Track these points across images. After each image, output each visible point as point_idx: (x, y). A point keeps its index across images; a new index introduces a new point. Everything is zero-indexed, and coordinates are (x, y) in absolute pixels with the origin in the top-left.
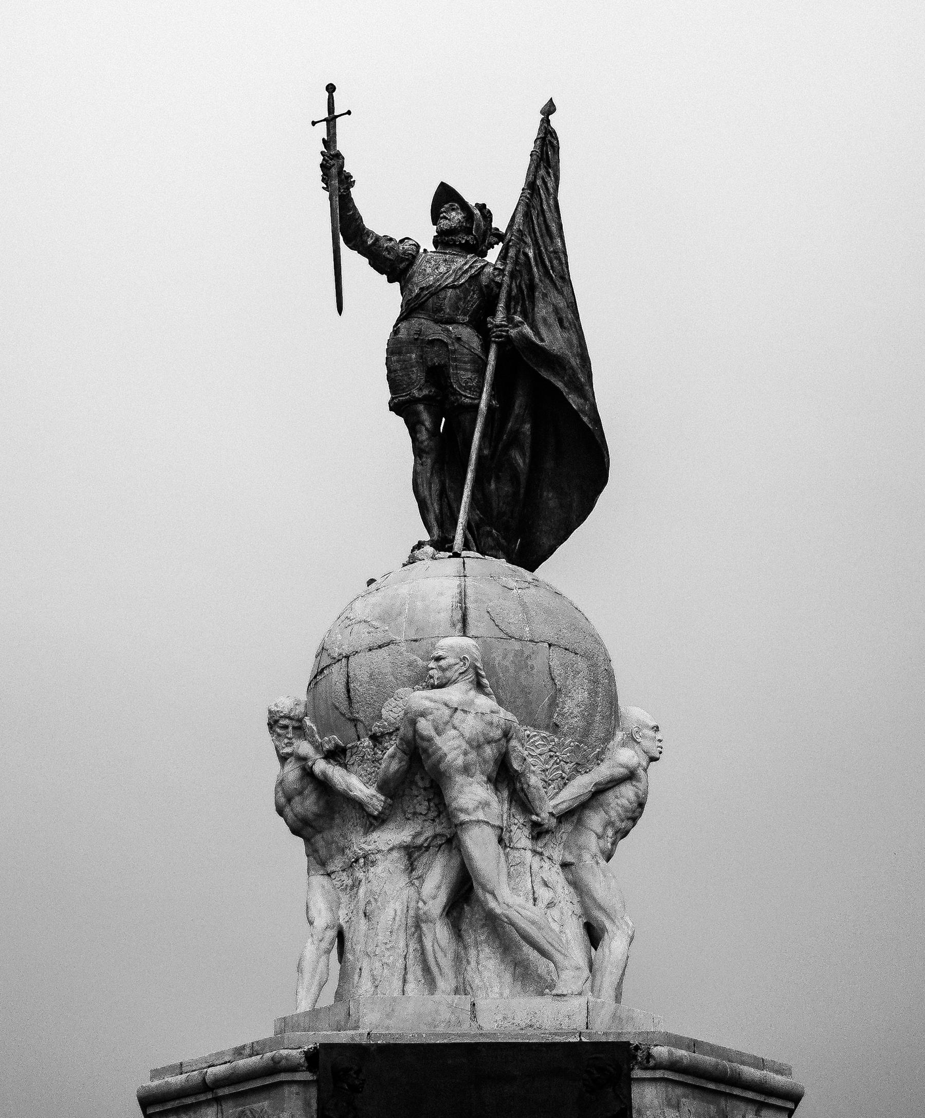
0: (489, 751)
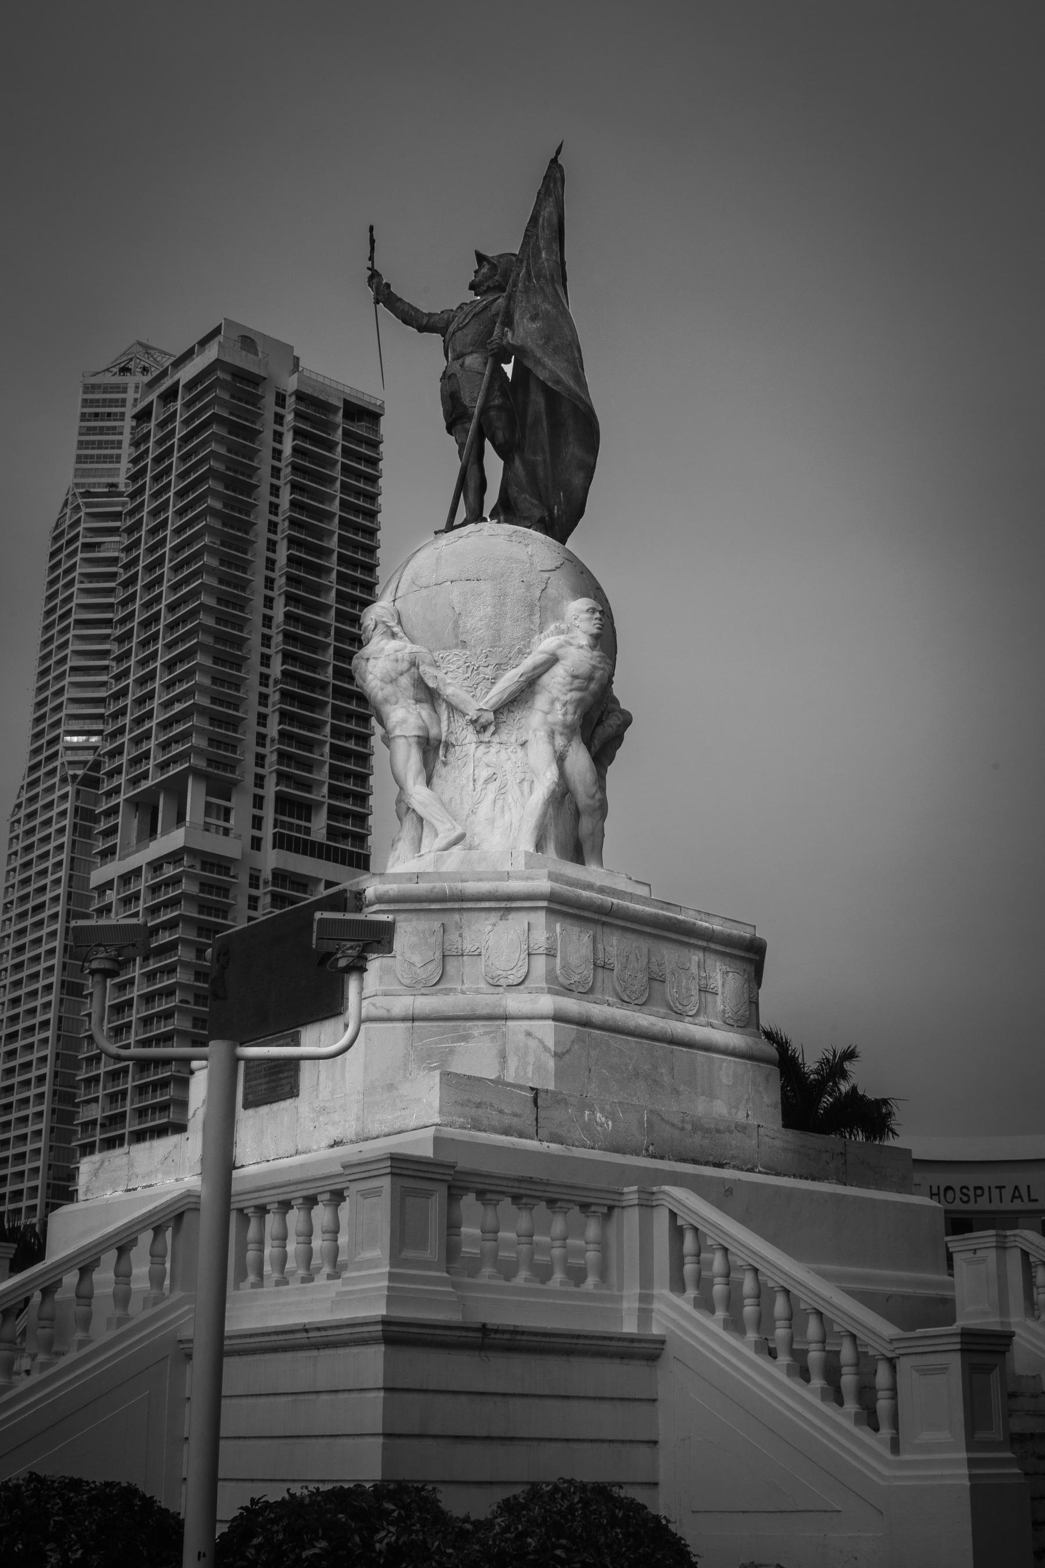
0: (405, 681)
